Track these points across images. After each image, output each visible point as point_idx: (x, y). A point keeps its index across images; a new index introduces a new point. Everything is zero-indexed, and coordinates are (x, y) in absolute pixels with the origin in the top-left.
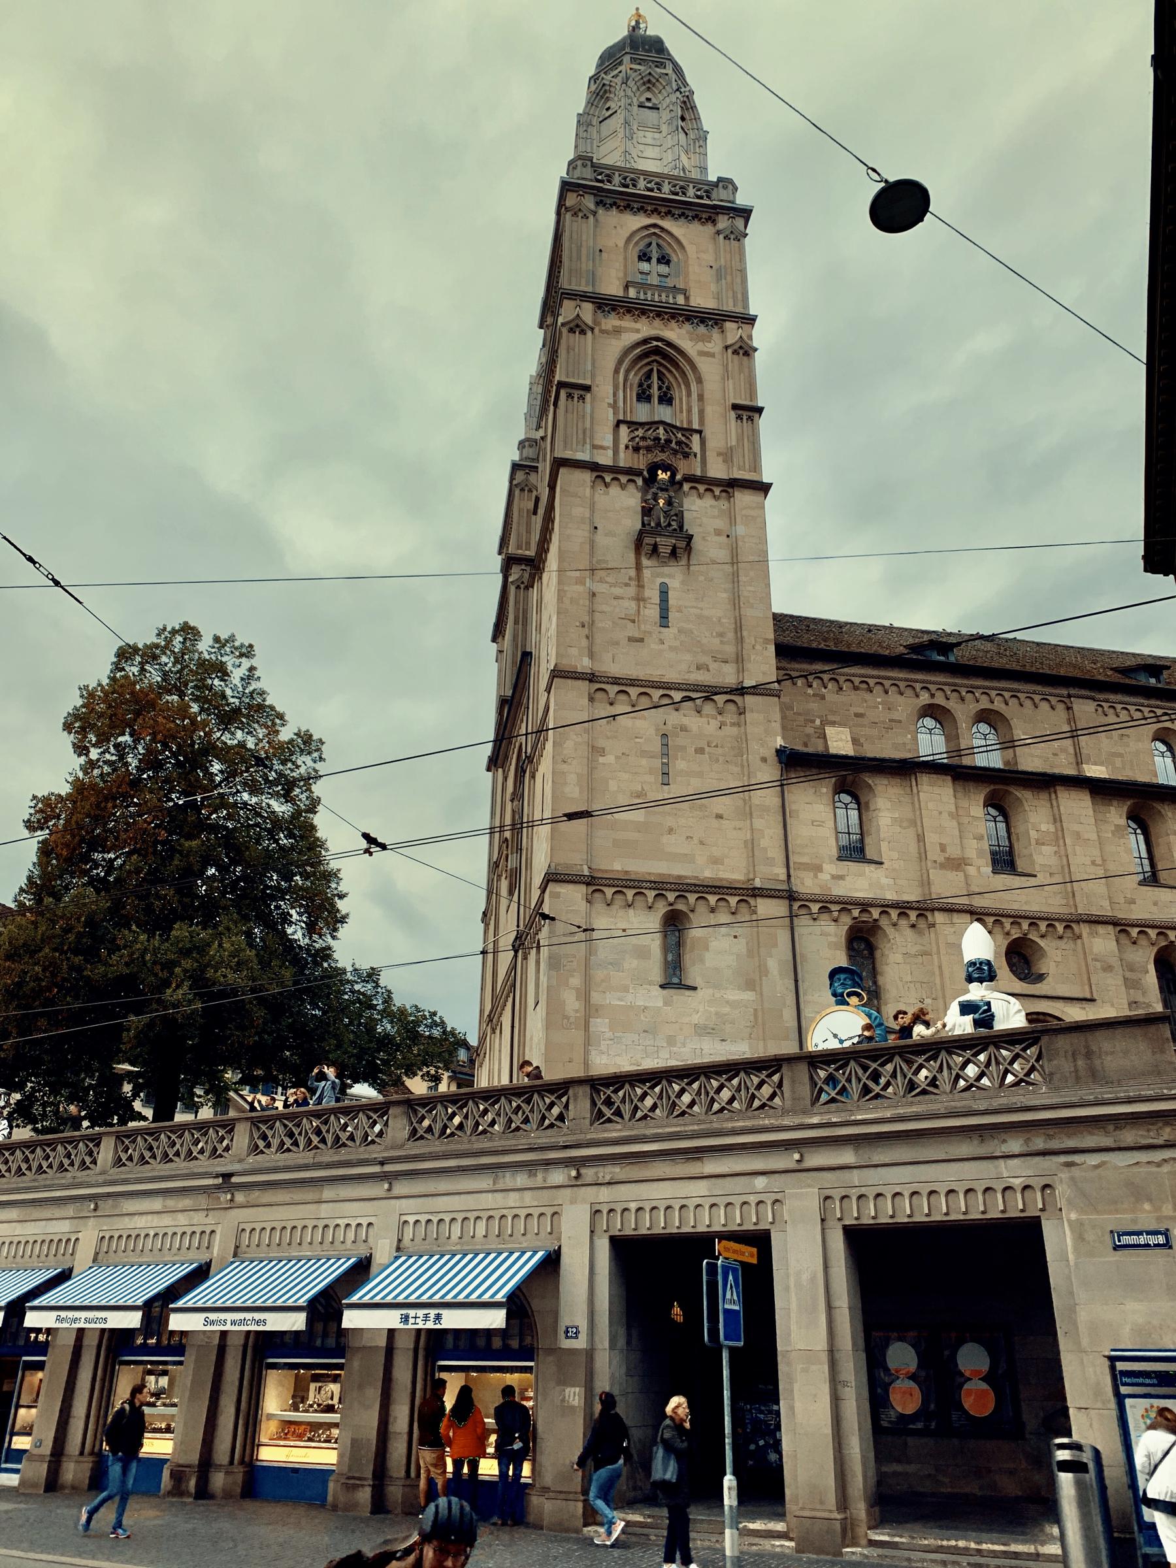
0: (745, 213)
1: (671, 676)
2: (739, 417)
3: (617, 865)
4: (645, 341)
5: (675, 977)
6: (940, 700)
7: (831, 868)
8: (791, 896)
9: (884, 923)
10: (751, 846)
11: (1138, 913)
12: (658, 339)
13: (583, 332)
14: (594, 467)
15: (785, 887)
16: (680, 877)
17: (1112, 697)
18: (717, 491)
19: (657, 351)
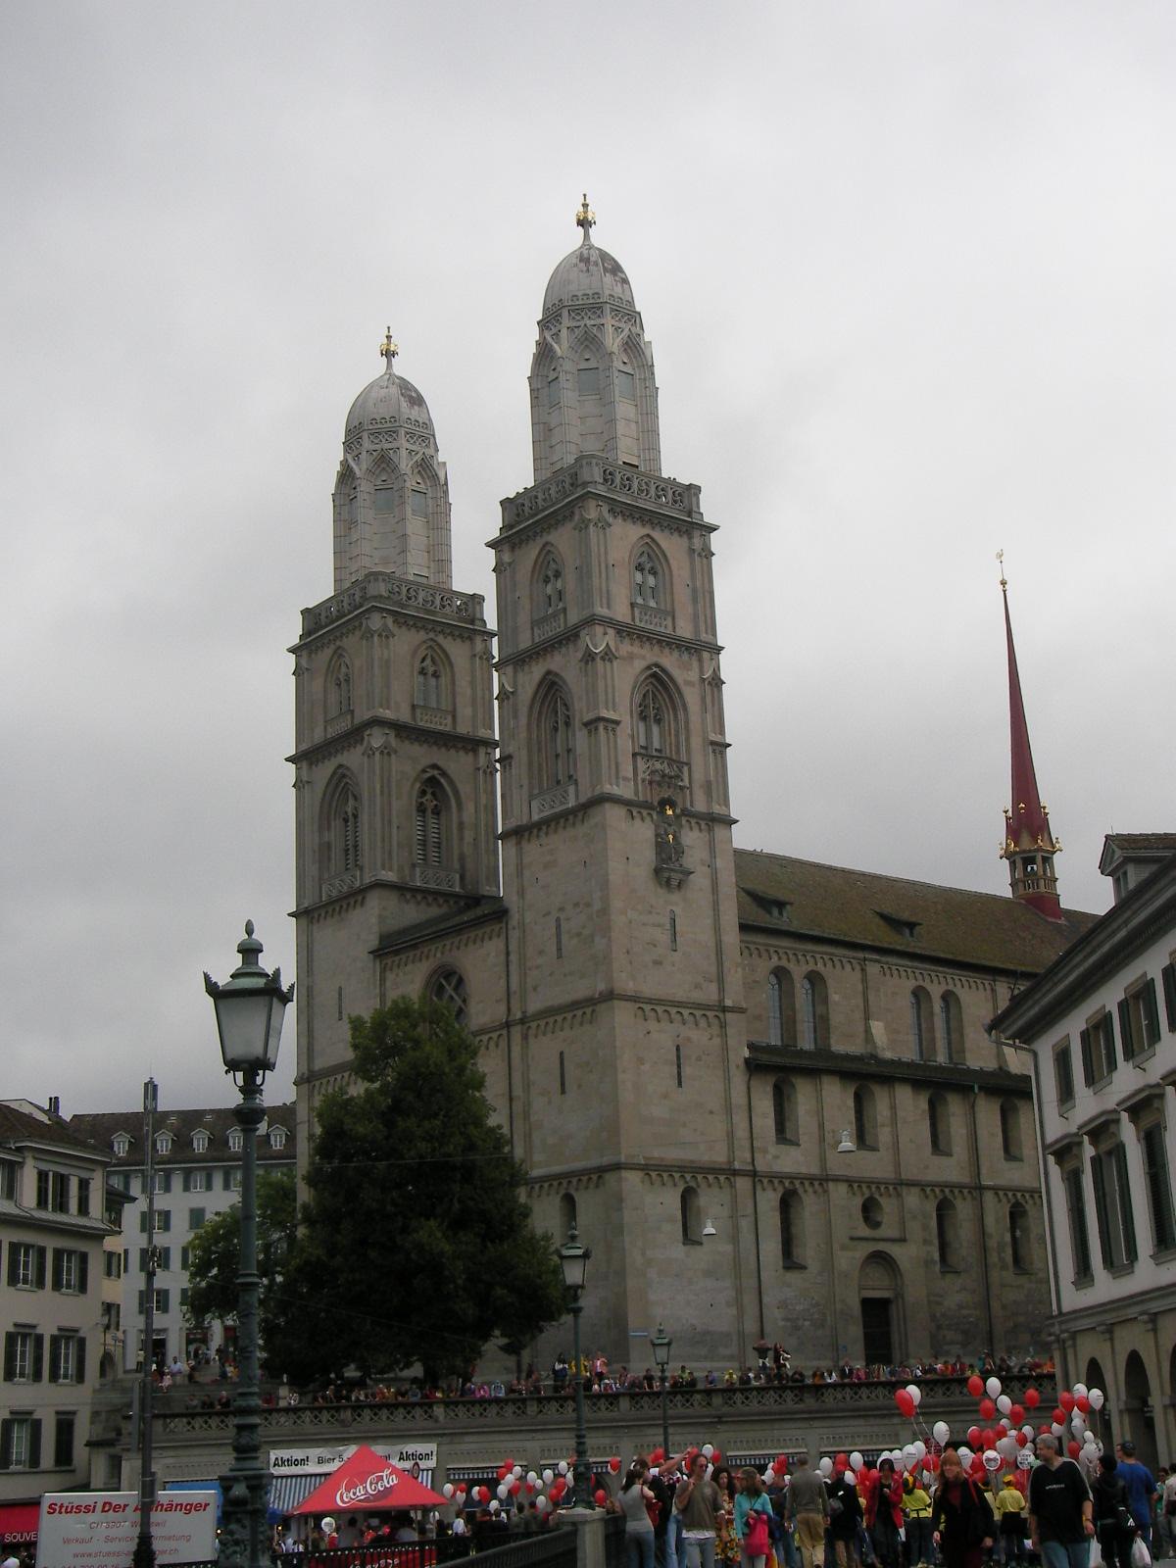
0: (713, 529)
1: (680, 995)
2: (714, 751)
3: (658, 1153)
4: (649, 668)
5: (690, 1235)
6: (784, 963)
7: (773, 1149)
8: (754, 1174)
9: (801, 1191)
10: (731, 1135)
11: (931, 1176)
12: (657, 665)
13: (610, 660)
14: (627, 803)
15: (750, 1168)
16: (692, 1162)
17: (890, 959)
18: (703, 823)
19: (654, 675)
